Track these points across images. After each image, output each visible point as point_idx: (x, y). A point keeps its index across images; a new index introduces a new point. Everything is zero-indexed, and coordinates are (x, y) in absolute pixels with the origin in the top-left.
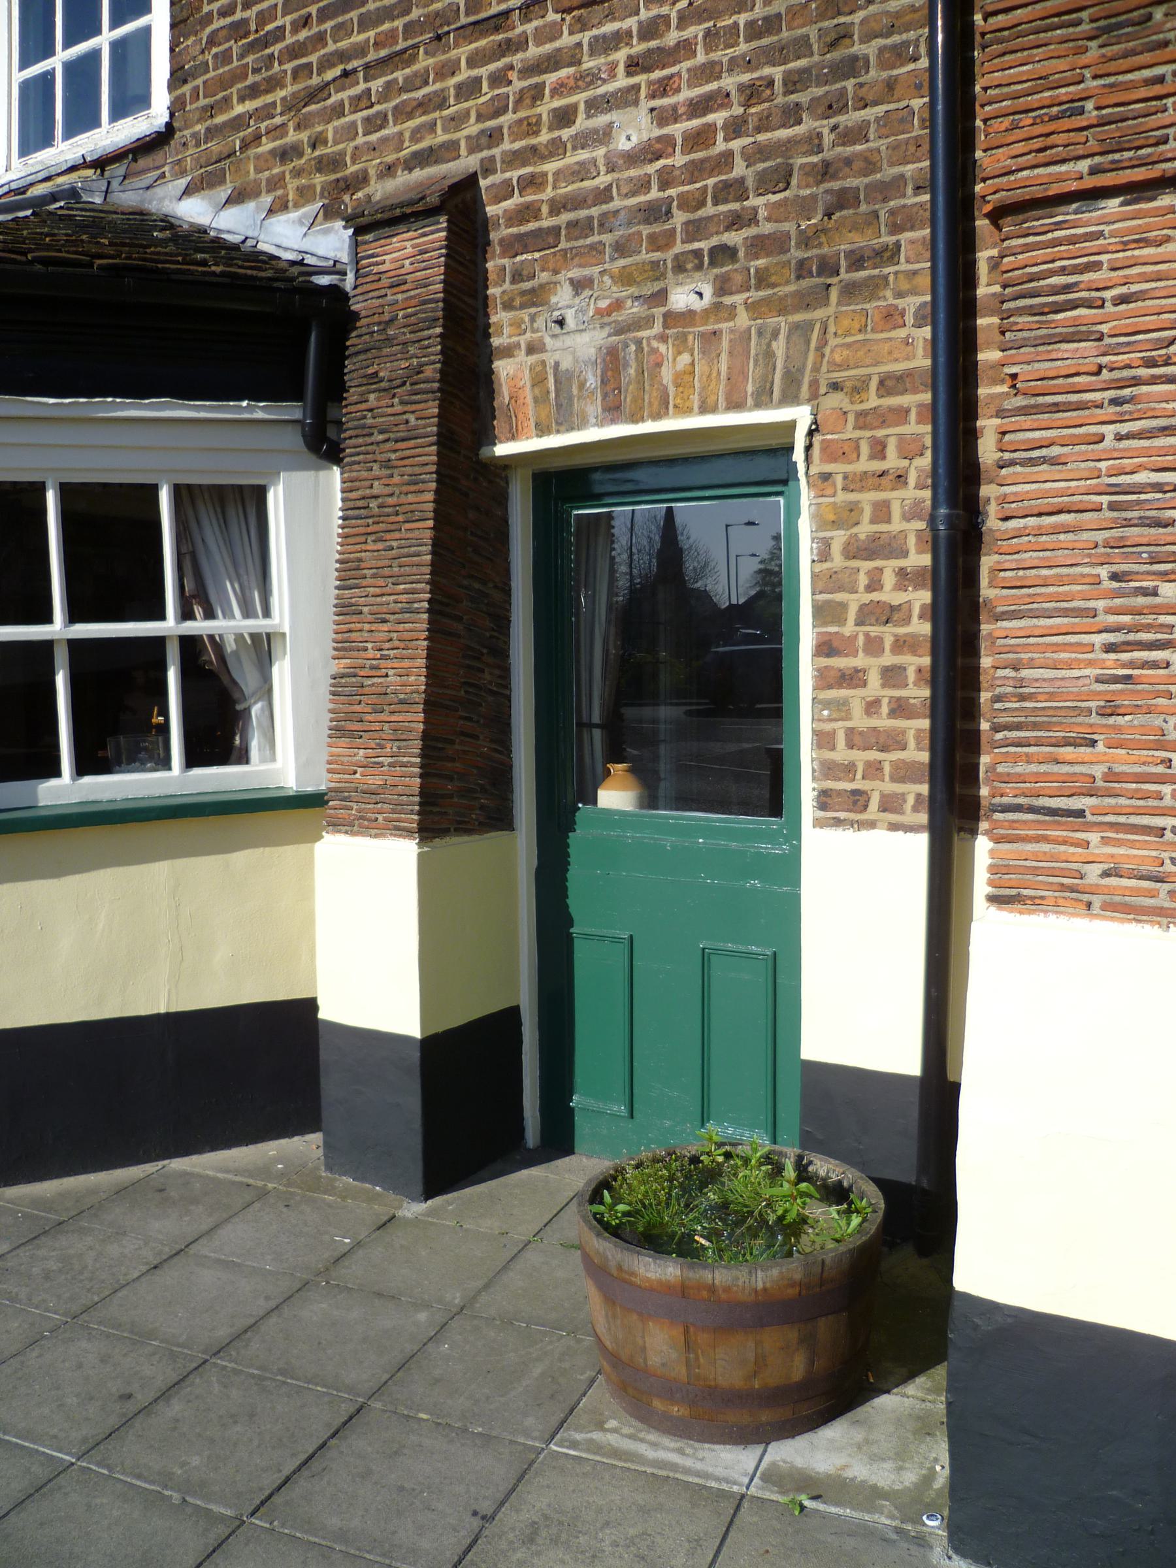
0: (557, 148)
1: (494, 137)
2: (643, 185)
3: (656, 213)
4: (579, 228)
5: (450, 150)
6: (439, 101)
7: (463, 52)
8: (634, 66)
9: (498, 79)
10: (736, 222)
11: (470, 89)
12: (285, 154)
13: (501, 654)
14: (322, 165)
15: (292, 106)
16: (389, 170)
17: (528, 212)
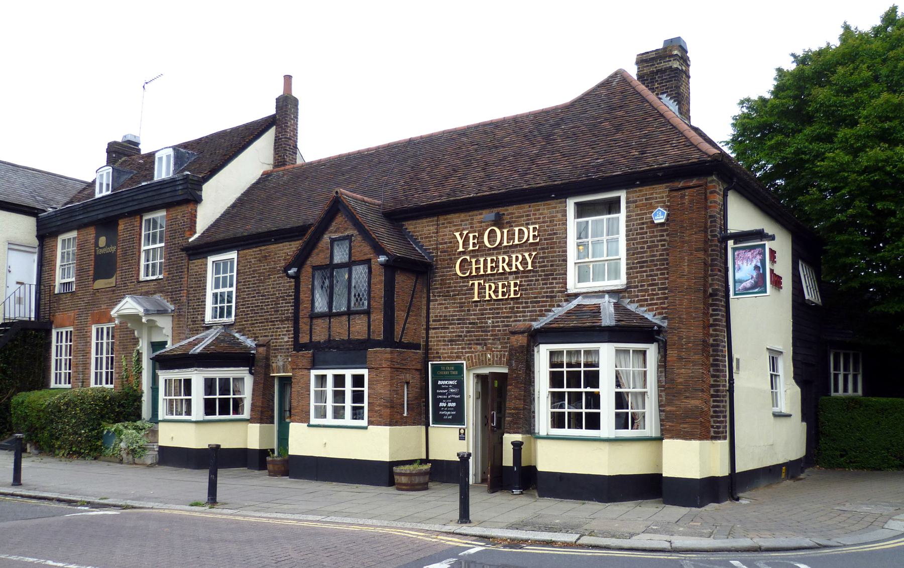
0: (279, 339)
1: (272, 336)
2: (287, 345)
3: (288, 349)
4: (281, 349)
7: (270, 324)
8: (287, 331)
9: (273, 328)
12: (249, 331)
13: (273, 401)
16: (261, 337)
17: (276, 346)
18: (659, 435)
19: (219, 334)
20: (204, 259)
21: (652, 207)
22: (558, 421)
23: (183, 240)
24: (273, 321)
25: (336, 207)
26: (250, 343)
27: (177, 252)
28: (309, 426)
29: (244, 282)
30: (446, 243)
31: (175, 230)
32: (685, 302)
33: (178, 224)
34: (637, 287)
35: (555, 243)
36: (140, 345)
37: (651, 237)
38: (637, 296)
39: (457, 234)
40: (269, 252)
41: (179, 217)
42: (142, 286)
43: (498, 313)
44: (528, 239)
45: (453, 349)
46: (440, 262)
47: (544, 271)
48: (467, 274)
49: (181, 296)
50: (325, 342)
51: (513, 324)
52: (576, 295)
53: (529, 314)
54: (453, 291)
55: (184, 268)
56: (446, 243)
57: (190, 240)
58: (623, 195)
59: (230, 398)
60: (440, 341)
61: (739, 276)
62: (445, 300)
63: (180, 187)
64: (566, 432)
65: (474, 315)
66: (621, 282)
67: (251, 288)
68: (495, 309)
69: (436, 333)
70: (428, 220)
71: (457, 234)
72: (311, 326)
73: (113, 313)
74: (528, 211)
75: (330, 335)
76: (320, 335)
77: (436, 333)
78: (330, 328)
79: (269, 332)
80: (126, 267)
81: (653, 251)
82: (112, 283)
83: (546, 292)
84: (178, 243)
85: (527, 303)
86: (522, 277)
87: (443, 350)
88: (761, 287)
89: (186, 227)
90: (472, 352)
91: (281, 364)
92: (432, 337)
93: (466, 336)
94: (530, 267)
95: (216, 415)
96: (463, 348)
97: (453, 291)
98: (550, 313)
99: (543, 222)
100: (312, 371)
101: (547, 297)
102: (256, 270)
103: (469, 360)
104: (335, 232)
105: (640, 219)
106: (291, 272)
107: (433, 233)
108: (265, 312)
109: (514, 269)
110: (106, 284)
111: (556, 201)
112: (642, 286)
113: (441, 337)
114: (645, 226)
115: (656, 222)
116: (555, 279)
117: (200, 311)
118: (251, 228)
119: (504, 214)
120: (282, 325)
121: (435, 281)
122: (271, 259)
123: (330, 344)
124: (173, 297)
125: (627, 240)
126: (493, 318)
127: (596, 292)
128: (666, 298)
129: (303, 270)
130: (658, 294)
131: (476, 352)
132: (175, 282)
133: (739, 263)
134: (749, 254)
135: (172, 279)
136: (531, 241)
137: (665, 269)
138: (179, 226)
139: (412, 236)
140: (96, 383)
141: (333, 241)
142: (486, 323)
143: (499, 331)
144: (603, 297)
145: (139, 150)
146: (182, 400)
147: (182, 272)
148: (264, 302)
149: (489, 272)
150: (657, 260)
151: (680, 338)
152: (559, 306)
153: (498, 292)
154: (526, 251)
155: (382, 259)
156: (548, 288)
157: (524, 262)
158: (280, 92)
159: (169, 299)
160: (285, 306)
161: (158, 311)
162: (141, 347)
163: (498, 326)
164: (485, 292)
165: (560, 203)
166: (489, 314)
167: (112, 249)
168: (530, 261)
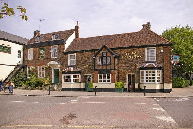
22: (147, 81)
25: (104, 47)
58: (155, 48)
64: (149, 83)
73: (48, 64)
76: (100, 68)
155: (114, 56)
158: (76, 25)
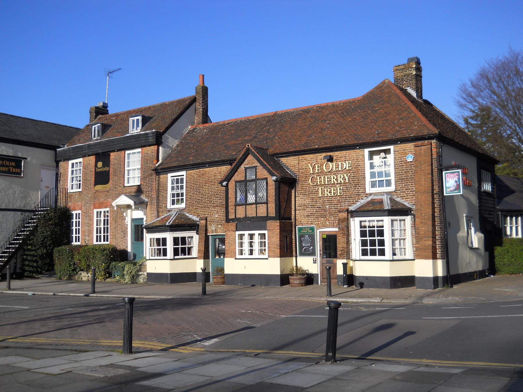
0: (212, 216)
1: (208, 214)
3: (218, 221)
5: (206, 215)
6: (205, 211)
8: (217, 212)
9: (209, 211)
10: (222, 222)
11: (207, 211)
12: (194, 212)
14: (197, 213)
15: (195, 209)
16: (202, 215)
18: (413, 258)
19: (177, 214)
20: (165, 175)
21: (406, 154)
22: (364, 253)
23: (152, 165)
24: (209, 207)
26: (195, 218)
27: (149, 171)
28: (236, 259)
29: (191, 187)
30: (303, 169)
31: (147, 159)
32: (423, 197)
33: (149, 156)
34: (400, 190)
35: (360, 170)
36: (127, 220)
37: (406, 168)
38: (400, 195)
39: (309, 165)
40: (205, 172)
41: (149, 153)
42: (127, 189)
43: (332, 203)
44: (345, 168)
45: (309, 219)
46: (300, 178)
47: (354, 183)
48: (315, 184)
49: (152, 194)
50: (243, 218)
51: (339, 208)
52: (371, 194)
53: (347, 203)
54: (308, 192)
55: (154, 180)
56: (303, 169)
57: (157, 165)
58: (392, 147)
59: (179, 247)
60: (302, 216)
61: (448, 185)
62: (304, 196)
63: (151, 138)
64: (369, 257)
65: (319, 203)
66: (392, 188)
67: (195, 190)
68: (330, 201)
69: (299, 212)
70: (294, 157)
71: (309, 165)
72: (235, 210)
73: (114, 204)
74: (345, 155)
75: (246, 215)
77: (299, 212)
78: (246, 211)
79: (206, 213)
80: (115, 178)
81: (407, 174)
82: (107, 187)
83: (356, 193)
84: (149, 166)
85: (345, 198)
86: (343, 186)
87: (304, 220)
88: (458, 190)
89: (154, 158)
90: (319, 221)
91: (214, 228)
92: (297, 214)
93: (316, 214)
94: (347, 181)
95: (179, 255)
96: (314, 219)
97: (308, 192)
98: (358, 203)
99: (353, 160)
100: (236, 232)
101: (356, 195)
102: (198, 181)
103: (317, 225)
104: (247, 164)
105: (401, 159)
106: (224, 184)
107: (297, 164)
108: (203, 203)
109: (339, 182)
110: (102, 188)
111: (359, 150)
112: (402, 190)
113: (302, 214)
114: (403, 162)
115: (408, 161)
116: (360, 186)
117: (164, 202)
118: (192, 160)
119: (333, 156)
120: (214, 209)
121: (299, 187)
122: (207, 175)
123: (246, 218)
124: (147, 195)
125: (395, 169)
126: (329, 205)
127: (380, 193)
128: (414, 195)
129: (230, 183)
130: (410, 194)
131: (321, 221)
132: (148, 187)
133: (448, 179)
134: (452, 175)
135: (146, 185)
136: (347, 168)
137: (413, 182)
138: (149, 157)
139: (286, 165)
140: (97, 241)
141: (246, 169)
142: (326, 207)
143: (333, 211)
144: (384, 195)
145: (107, 111)
146: (155, 249)
147: (152, 182)
148: (203, 197)
149: (326, 183)
150: (409, 178)
151: (422, 214)
152: (362, 199)
153: (331, 193)
154: (345, 173)
156: (356, 191)
157: (344, 179)
159: (144, 196)
160: (215, 200)
161: (140, 202)
162: (127, 222)
163: (332, 209)
164: (325, 193)
165: (361, 151)
166: (327, 203)
167: (106, 169)
168: (347, 178)
